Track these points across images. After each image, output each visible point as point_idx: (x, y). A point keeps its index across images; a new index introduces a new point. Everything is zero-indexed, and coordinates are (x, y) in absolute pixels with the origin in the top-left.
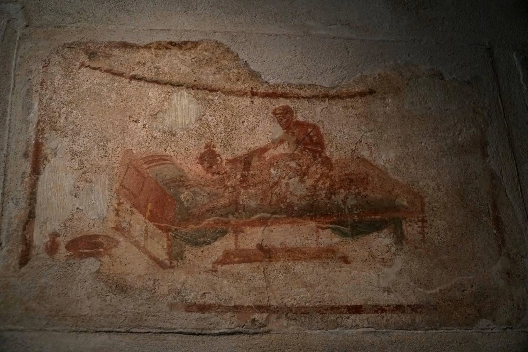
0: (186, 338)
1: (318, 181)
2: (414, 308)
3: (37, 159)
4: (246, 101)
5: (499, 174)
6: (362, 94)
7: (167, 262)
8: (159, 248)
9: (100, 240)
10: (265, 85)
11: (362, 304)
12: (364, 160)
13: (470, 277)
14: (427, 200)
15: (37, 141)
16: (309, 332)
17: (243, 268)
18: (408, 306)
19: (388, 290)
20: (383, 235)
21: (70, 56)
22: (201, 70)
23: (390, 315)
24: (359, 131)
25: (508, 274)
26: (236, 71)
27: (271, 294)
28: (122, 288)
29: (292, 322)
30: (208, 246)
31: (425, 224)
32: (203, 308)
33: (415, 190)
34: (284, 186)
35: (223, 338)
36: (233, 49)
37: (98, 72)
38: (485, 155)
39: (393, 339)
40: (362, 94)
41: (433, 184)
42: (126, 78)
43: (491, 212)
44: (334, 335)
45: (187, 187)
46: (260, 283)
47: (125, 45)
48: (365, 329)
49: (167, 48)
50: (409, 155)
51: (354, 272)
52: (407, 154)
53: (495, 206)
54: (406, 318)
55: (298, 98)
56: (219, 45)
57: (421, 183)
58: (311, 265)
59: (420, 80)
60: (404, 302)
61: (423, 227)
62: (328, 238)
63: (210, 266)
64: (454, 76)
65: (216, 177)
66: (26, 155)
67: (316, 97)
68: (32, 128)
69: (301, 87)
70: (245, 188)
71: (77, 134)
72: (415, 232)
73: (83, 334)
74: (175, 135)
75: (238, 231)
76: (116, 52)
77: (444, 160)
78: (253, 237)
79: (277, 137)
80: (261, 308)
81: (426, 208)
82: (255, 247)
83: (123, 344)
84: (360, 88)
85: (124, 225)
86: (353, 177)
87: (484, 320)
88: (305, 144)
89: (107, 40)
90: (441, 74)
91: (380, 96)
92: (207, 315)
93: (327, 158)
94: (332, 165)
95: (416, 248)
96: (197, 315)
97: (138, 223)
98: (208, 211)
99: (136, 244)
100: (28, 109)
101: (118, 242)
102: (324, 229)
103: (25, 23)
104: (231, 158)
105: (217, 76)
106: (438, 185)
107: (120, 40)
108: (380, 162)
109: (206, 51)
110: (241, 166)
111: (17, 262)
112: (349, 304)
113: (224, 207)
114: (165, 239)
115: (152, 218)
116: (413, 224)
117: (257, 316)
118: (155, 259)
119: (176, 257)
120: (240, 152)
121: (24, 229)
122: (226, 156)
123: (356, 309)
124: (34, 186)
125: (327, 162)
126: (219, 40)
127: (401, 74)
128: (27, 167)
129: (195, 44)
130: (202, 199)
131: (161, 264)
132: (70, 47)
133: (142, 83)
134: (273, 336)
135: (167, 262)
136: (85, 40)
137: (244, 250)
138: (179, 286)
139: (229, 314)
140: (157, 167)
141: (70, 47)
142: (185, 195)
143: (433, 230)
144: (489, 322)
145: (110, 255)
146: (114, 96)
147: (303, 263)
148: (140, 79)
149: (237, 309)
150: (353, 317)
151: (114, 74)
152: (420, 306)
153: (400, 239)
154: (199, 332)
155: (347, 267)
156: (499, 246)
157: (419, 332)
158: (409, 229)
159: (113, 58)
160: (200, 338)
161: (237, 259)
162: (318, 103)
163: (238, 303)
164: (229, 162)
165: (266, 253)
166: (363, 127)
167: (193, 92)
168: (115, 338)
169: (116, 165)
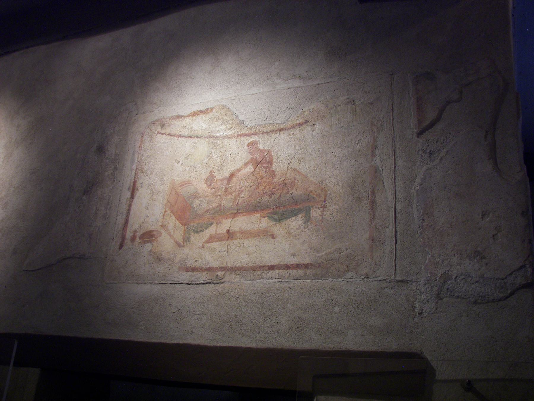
0: (184, 286)
1: (266, 187)
2: (306, 266)
3: (133, 190)
4: (235, 140)
5: (380, 169)
6: (300, 125)
7: (182, 243)
8: (179, 236)
9: (154, 233)
10: (245, 128)
11: (277, 264)
12: (295, 170)
13: (347, 244)
14: (329, 192)
15: (134, 180)
16: (245, 282)
17: (216, 245)
18: (304, 264)
19: (293, 255)
20: (298, 218)
21: (153, 128)
22: (213, 125)
23: (291, 271)
24: (294, 150)
25: (373, 240)
26: (231, 122)
27: (228, 260)
28: (159, 259)
29: (238, 276)
30: (203, 233)
31: (325, 209)
32: (194, 269)
33: (323, 186)
34: (247, 192)
35: (201, 286)
36: (232, 108)
37: (164, 135)
38: (373, 155)
39: (291, 285)
40: (300, 125)
41: (334, 181)
42: (176, 136)
43: (370, 197)
44: (258, 284)
45: (197, 198)
46: (224, 253)
47: (178, 117)
48: (276, 280)
49: (198, 115)
50: (322, 162)
51: (276, 244)
52: (322, 162)
53: (373, 193)
54: (301, 272)
55: (262, 134)
56: (224, 106)
57: (327, 181)
58: (253, 240)
59: (339, 108)
60: (302, 262)
61: (323, 211)
62: (265, 223)
63: (201, 245)
64: (362, 100)
65: (213, 190)
66: (129, 189)
67: (272, 131)
68: (134, 172)
69: (264, 126)
70: (226, 196)
71: (152, 174)
72: (317, 215)
73: (140, 285)
74: (195, 167)
75: (218, 223)
76: (174, 122)
77: (345, 163)
78: (226, 224)
79: (247, 161)
80: (221, 269)
81: (327, 198)
82: (225, 232)
83: (156, 290)
84: (301, 120)
85: (166, 224)
86: (286, 182)
87: (350, 273)
88: (262, 164)
89: (170, 115)
90: (354, 101)
91: (311, 124)
92: (195, 273)
93: (273, 171)
94: (275, 175)
95: (316, 225)
96: (190, 273)
97: (172, 221)
98: (206, 211)
99: (170, 235)
100: (132, 162)
101: (161, 233)
102: (264, 217)
103: (137, 113)
104: (221, 178)
105: (221, 127)
106: (338, 181)
107: (176, 114)
108: (304, 171)
109: (217, 112)
110: (225, 182)
111: (118, 247)
112: (270, 264)
113: (214, 208)
114: (183, 230)
115: (179, 218)
116: (317, 210)
117: (220, 273)
118: (176, 242)
119: (187, 240)
120: (227, 174)
121: (123, 229)
122: (219, 176)
123: (272, 268)
124: (130, 205)
125: (273, 174)
126: (224, 104)
127: (327, 106)
128: (129, 195)
129: (212, 109)
130: (204, 205)
131: (179, 245)
132: (154, 123)
133: (183, 139)
134: (226, 285)
135: (182, 243)
136: (161, 117)
137: (219, 234)
138: (185, 257)
139: (206, 272)
140: (185, 189)
141: (154, 123)
142: (196, 203)
143: (329, 213)
144: (353, 274)
145: (157, 241)
146: (170, 149)
147: (250, 240)
148: (182, 137)
149: (210, 269)
150: (271, 272)
151: (171, 136)
152: (311, 264)
153: (308, 220)
154: (190, 283)
155: (272, 241)
156: (371, 221)
157: (307, 281)
158: (314, 213)
159: (172, 126)
160: (191, 285)
161: (215, 240)
162: (273, 135)
163: (211, 266)
164: (221, 180)
165: (230, 235)
166: (297, 148)
167: (207, 140)
168: (154, 286)
169: (166, 189)
